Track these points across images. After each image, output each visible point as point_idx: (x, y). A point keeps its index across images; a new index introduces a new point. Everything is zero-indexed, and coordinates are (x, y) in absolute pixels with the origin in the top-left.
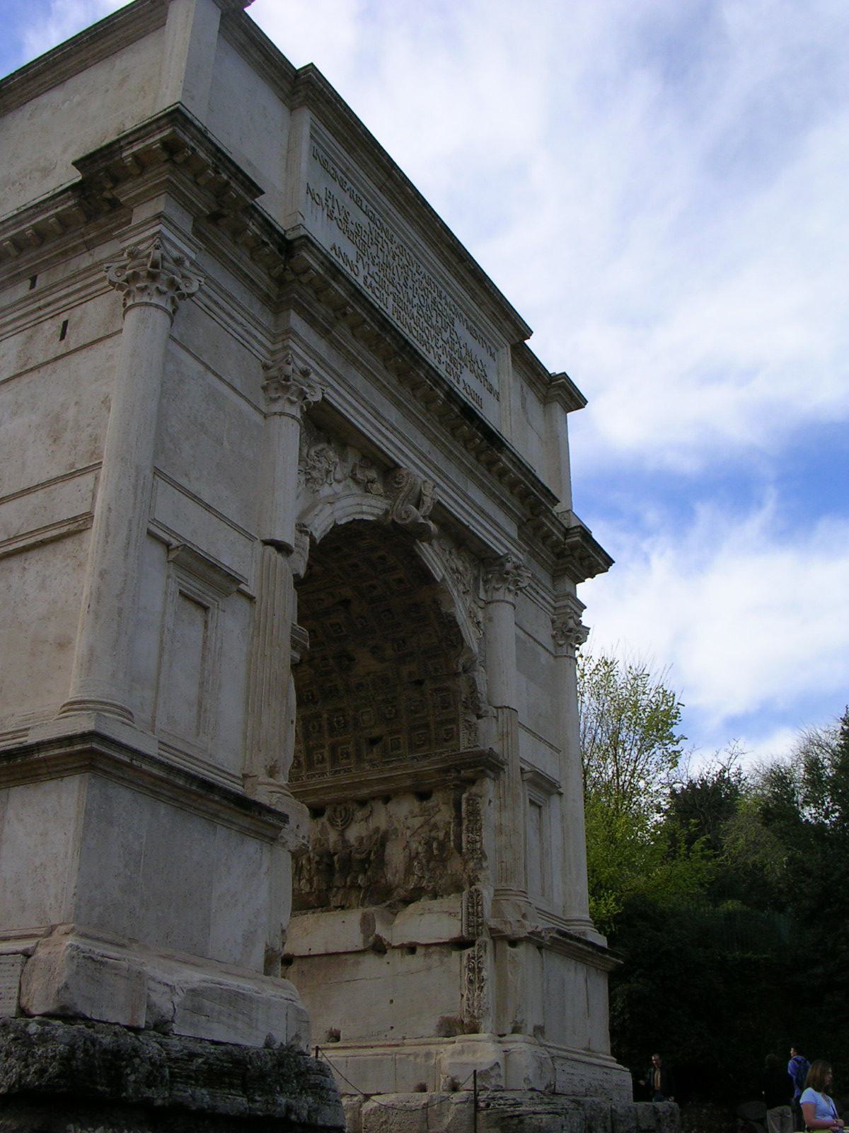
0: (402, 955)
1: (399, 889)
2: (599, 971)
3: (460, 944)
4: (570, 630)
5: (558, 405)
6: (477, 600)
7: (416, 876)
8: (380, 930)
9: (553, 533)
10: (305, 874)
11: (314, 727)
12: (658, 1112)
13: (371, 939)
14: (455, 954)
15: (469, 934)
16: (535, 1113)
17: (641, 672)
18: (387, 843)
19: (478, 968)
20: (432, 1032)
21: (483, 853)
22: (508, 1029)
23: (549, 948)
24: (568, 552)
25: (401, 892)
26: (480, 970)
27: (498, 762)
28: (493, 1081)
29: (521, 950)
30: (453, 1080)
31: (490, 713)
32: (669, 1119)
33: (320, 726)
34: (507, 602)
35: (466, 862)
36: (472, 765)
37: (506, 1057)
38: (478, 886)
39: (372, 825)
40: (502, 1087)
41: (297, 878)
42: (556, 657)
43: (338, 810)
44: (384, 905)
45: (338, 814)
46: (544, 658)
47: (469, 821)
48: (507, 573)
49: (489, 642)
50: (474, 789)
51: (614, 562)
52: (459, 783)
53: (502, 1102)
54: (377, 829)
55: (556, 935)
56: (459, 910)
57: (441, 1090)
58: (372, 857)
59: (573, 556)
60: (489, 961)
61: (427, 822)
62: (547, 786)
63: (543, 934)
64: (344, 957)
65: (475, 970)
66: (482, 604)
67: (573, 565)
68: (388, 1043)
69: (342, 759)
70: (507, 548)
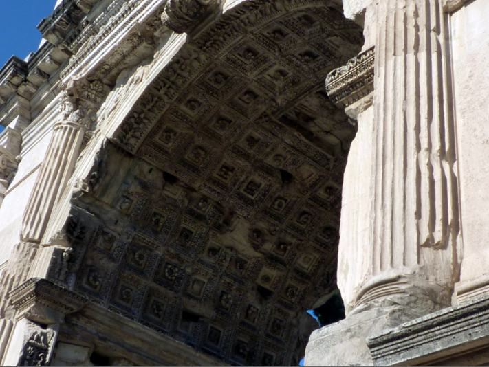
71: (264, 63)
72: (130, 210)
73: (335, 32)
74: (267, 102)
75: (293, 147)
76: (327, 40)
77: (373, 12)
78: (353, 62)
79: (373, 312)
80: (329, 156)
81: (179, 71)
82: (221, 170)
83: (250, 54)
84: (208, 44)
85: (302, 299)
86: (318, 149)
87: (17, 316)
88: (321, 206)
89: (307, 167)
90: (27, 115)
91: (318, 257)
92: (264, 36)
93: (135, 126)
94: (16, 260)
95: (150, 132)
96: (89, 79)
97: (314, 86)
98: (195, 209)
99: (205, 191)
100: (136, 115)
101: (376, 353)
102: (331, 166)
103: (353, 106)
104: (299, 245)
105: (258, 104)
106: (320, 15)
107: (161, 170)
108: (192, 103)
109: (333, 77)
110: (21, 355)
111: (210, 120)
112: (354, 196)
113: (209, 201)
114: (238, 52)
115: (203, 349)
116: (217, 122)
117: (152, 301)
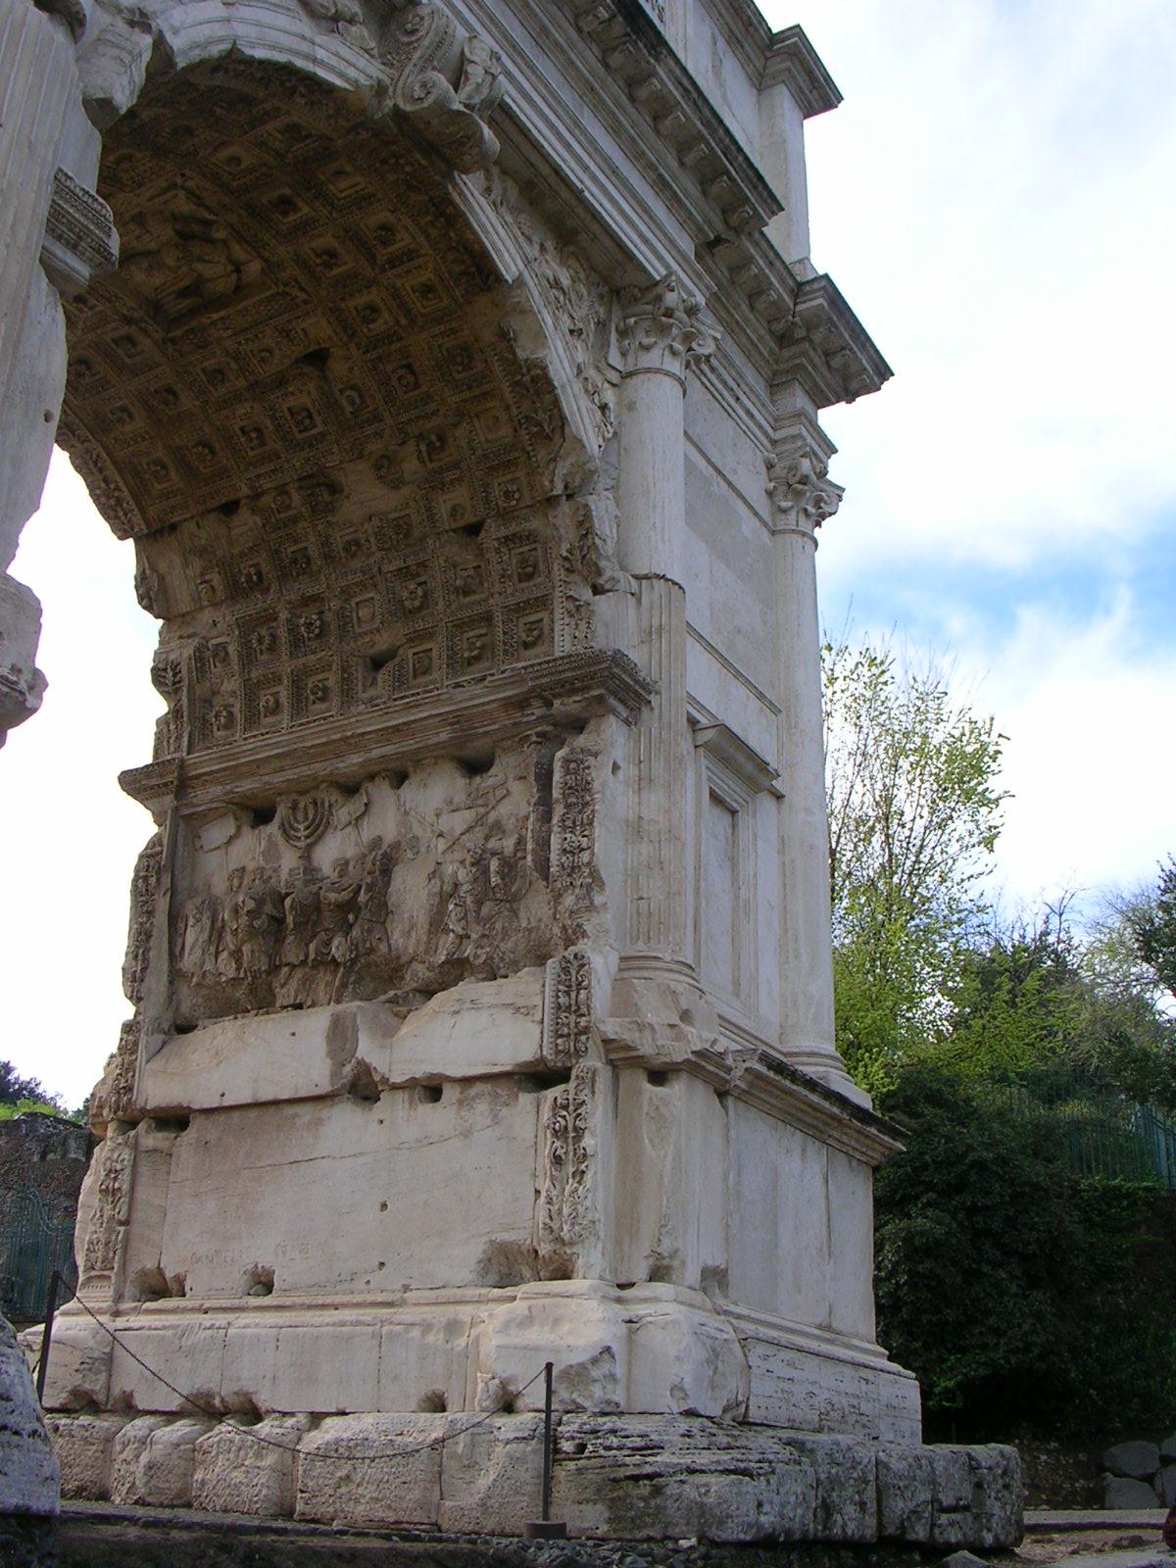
0: (411, 1103)
1: (415, 965)
2: (854, 1163)
3: (539, 1077)
4: (804, 481)
5: (785, 88)
6: (601, 365)
7: (451, 935)
8: (367, 1049)
9: (771, 283)
10: (229, 940)
11: (260, 641)
12: (979, 1467)
13: (348, 1069)
14: (526, 1099)
15: (558, 1052)
16: (692, 1471)
17: (932, 688)
18: (396, 868)
19: (576, 1129)
20: (466, 1274)
21: (595, 875)
22: (641, 1270)
23: (744, 1097)
24: (800, 333)
25: (420, 972)
26: (579, 1132)
27: (637, 682)
28: (597, 1391)
29: (677, 1093)
30: (503, 1385)
31: (622, 585)
32: (1000, 1481)
33: (273, 637)
34: (667, 374)
35: (558, 897)
36: (578, 685)
37: (630, 1339)
38: (582, 946)
39: (368, 832)
40: (617, 1405)
41: (212, 949)
42: (773, 533)
43: (302, 805)
44: (382, 998)
45: (300, 816)
46: (749, 526)
47: (568, 806)
48: (669, 314)
49: (625, 449)
50: (581, 741)
51: (893, 375)
52: (549, 728)
53: (615, 1441)
54: (377, 842)
55: (758, 1067)
56: (537, 1001)
57: (477, 1408)
58: (362, 897)
59: (811, 342)
60: (599, 1112)
61: (480, 820)
62: (749, 768)
63: (729, 1061)
64: (290, 1110)
65: (568, 1133)
66: (614, 377)
67: (811, 361)
68: (370, 1298)
69: (314, 703)
70: (667, 267)
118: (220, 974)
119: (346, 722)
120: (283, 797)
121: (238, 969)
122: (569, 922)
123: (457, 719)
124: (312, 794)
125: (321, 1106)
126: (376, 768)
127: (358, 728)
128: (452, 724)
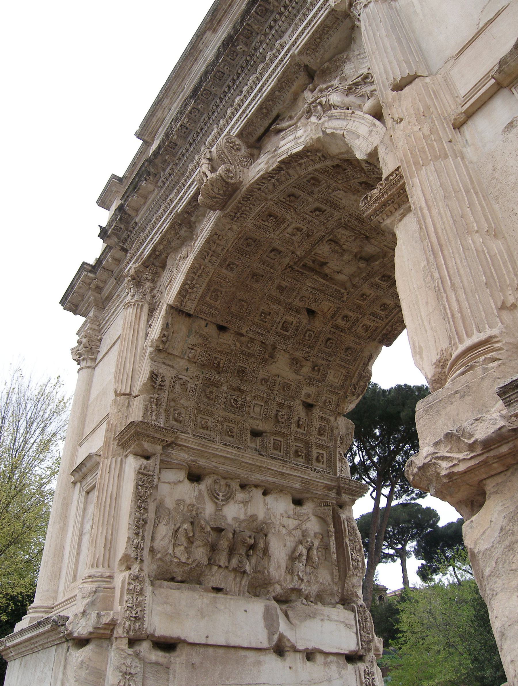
8: (283, 627)
14: (350, 666)
36: (353, 493)
41: (173, 542)
56: (354, 623)
64: (243, 653)
71: (284, 223)
72: (196, 359)
73: (339, 186)
74: (289, 255)
75: (314, 288)
76: (331, 195)
77: (385, 147)
78: (381, 185)
79: (479, 369)
80: (343, 291)
81: (218, 241)
82: (261, 315)
83: (272, 218)
84: (238, 215)
85: (338, 406)
86: (334, 286)
87: (125, 454)
88: (341, 331)
89: (326, 303)
90: (101, 305)
91: (344, 372)
92: (281, 201)
93: (190, 290)
94: (116, 411)
95: (202, 295)
96: (146, 265)
97: (325, 236)
98: (245, 350)
99: (251, 335)
100: (189, 282)
101: (508, 399)
102: (345, 299)
103: (388, 221)
104: (328, 365)
105: (282, 258)
106: (326, 174)
107: (215, 324)
108: (230, 267)
109: (366, 201)
110: (135, 482)
111: (247, 277)
112: (410, 290)
113: (255, 341)
114: (262, 218)
115: (270, 457)
116: (252, 278)
117: (225, 426)
118: (175, 557)
119: (266, 460)
120: (215, 476)
121: (188, 558)
122: (352, 590)
123: (305, 482)
124: (229, 481)
125: (259, 654)
126: (263, 484)
127: (269, 465)
128: (302, 483)
